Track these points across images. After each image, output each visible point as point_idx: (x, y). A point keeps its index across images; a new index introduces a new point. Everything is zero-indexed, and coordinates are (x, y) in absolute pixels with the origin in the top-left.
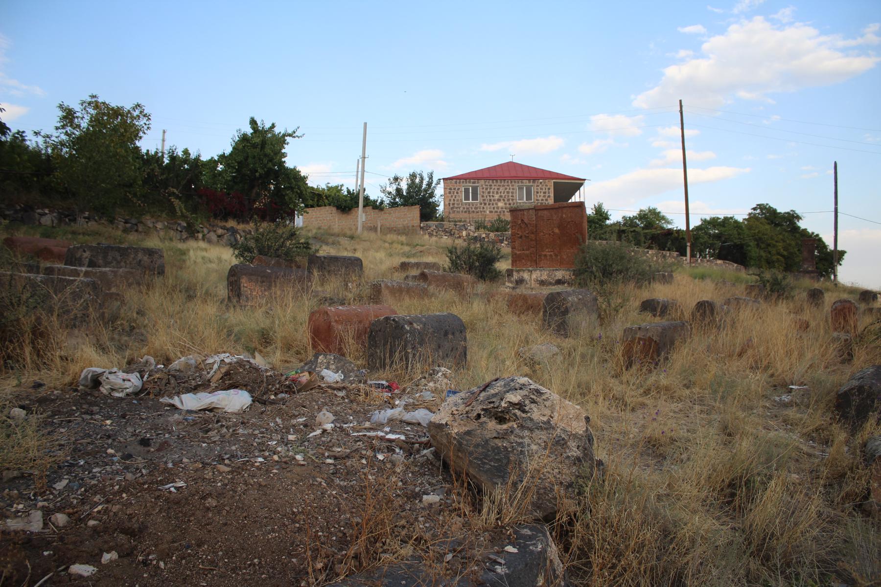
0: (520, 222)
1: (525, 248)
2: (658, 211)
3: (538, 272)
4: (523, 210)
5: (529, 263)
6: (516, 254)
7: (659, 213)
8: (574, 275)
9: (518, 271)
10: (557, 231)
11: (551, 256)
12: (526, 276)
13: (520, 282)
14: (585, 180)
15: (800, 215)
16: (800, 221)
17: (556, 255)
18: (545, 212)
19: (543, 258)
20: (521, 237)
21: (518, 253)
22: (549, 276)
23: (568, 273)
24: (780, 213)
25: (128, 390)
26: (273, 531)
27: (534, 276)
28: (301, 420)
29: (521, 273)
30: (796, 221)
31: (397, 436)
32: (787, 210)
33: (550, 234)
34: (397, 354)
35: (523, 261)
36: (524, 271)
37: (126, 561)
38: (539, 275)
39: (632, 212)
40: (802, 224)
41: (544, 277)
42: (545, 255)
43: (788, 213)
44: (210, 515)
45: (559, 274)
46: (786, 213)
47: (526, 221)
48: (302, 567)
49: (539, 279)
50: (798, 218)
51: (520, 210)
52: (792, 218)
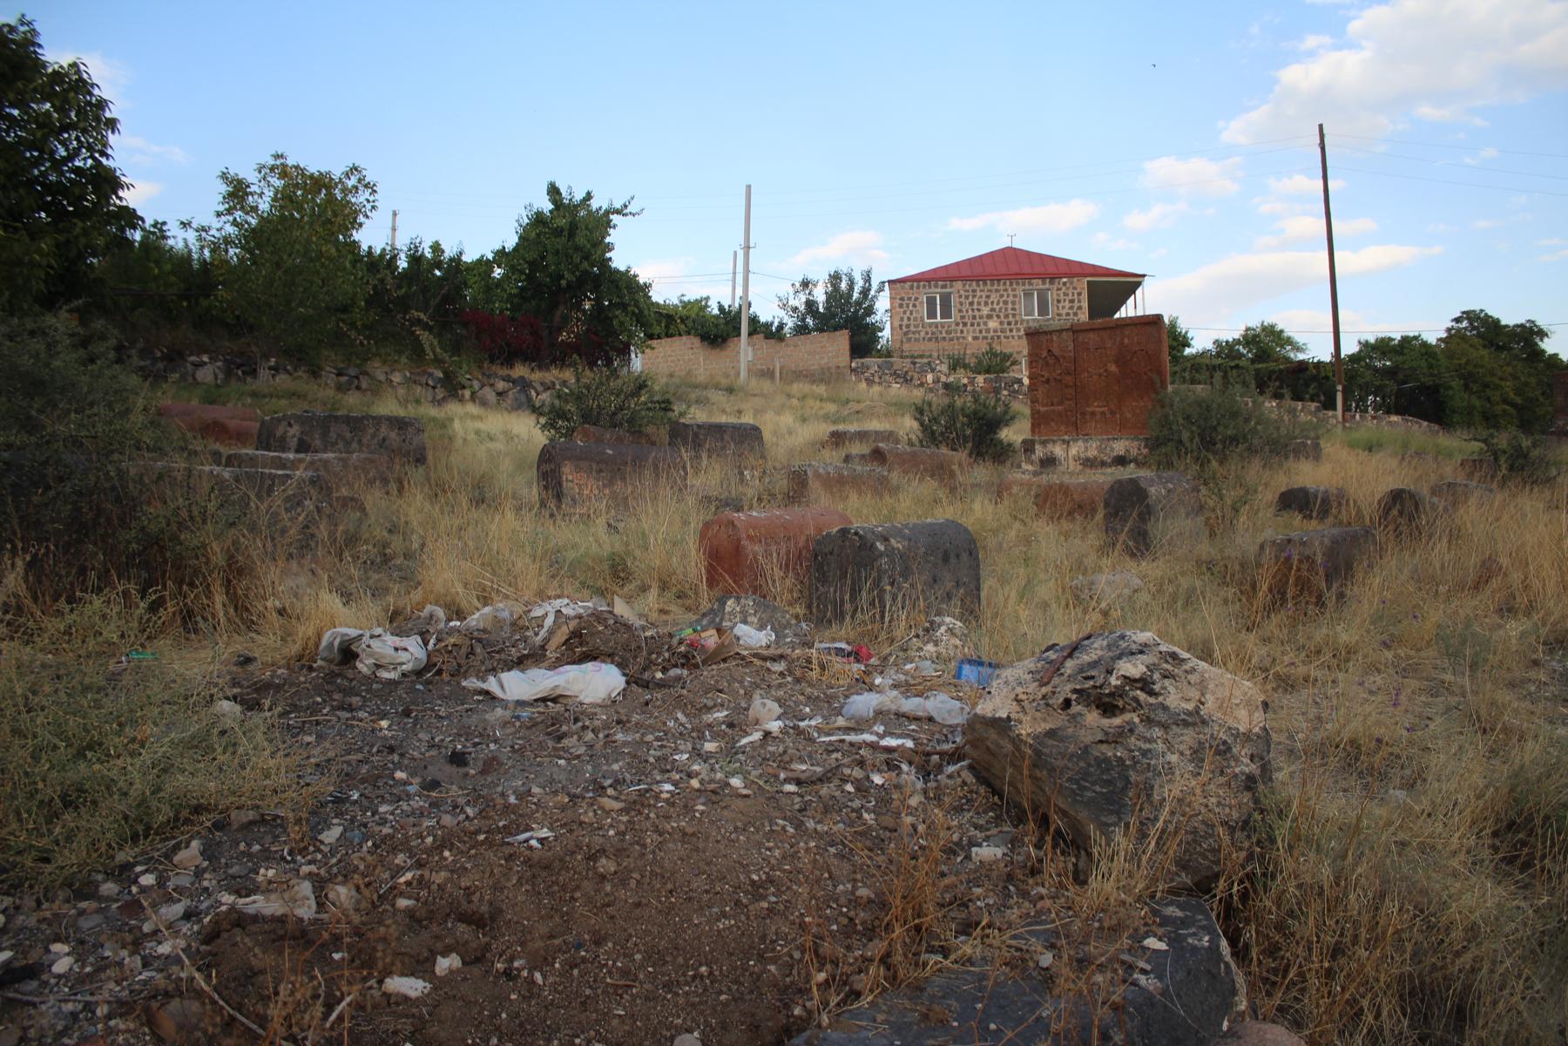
0: (1045, 354)
1: (1055, 400)
2: (1279, 328)
3: (1080, 443)
4: (1051, 332)
5: (1063, 428)
6: (1039, 412)
7: (1282, 331)
8: (1146, 446)
9: (1044, 443)
10: (1113, 368)
11: (1103, 413)
12: (1058, 450)
13: (1049, 462)
14: (1144, 276)
15: (1545, 328)
16: (1546, 339)
17: (1113, 413)
18: (1091, 335)
20: (1048, 381)
21: (1043, 409)
22: (1100, 450)
23: (1136, 443)
24: (1507, 326)
25: (404, 667)
26: (724, 915)
27: (1073, 451)
28: (720, 715)
29: (1050, 446)
30: (1538, 340)
31: (899, 742)
32: (1521, 320)
33: (1100, 375)
34: (864, 593)
35: (1053, 424)
37: (476, 970)
39: (1231, 331)
40: (1548, 346)
41: (1092, 453)
42: (1093, 414)
43: (1522, 326)
44: (608, 888)
45: (1120, 447)
46: (1517, 326)
47: (1056, 351)
48: (788, 979)
49: (1082, 455)
50: (1542, 334)
51: (1045, 333)
52: (1529, 335)
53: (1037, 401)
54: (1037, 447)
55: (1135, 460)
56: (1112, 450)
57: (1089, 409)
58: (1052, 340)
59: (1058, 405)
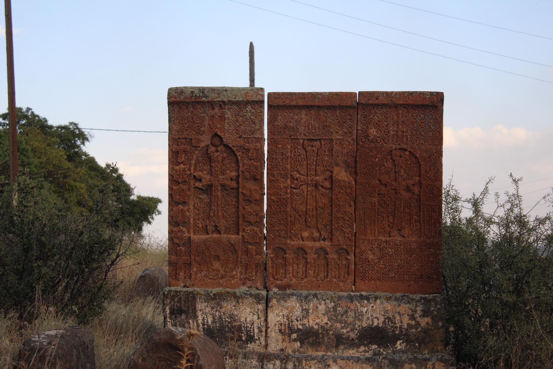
0: (205, 140)
1: (222, 224)
3: (293, 303)
5: (238, 272)
8: (425, 313)
17: (342, 252)
18: (303, 116)
19: (290, 256)
22: (333, 314)
23: (405, 308)
29: (228, 306)
33: (316, 186)
35: (217, 265)
36: (237, 298)
38: (298, 312)
42: (302, 250)
47: (230, 138)
49: (298, 325)
51: (212, 104)
53: (185, 223)
54: (200, 305)
55: (406, 336)
56: (359, 316)
57: (295, 243)
58: (222, 118)
59: (227, 231)
